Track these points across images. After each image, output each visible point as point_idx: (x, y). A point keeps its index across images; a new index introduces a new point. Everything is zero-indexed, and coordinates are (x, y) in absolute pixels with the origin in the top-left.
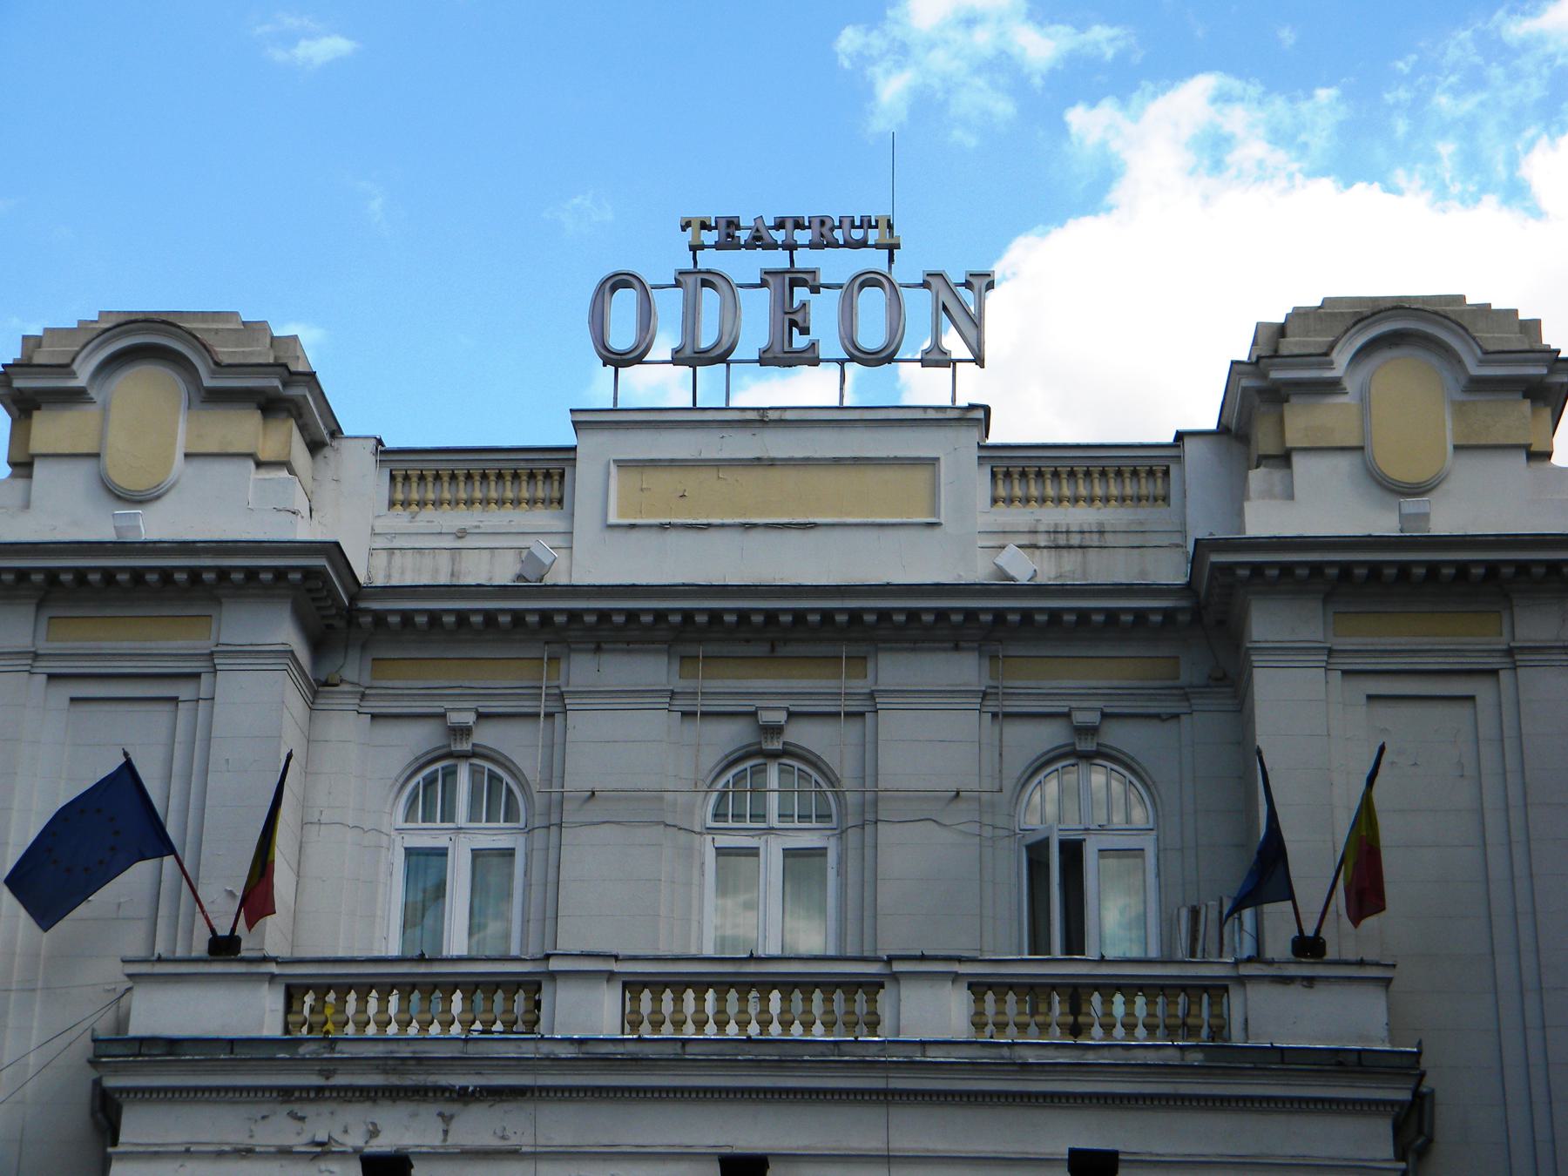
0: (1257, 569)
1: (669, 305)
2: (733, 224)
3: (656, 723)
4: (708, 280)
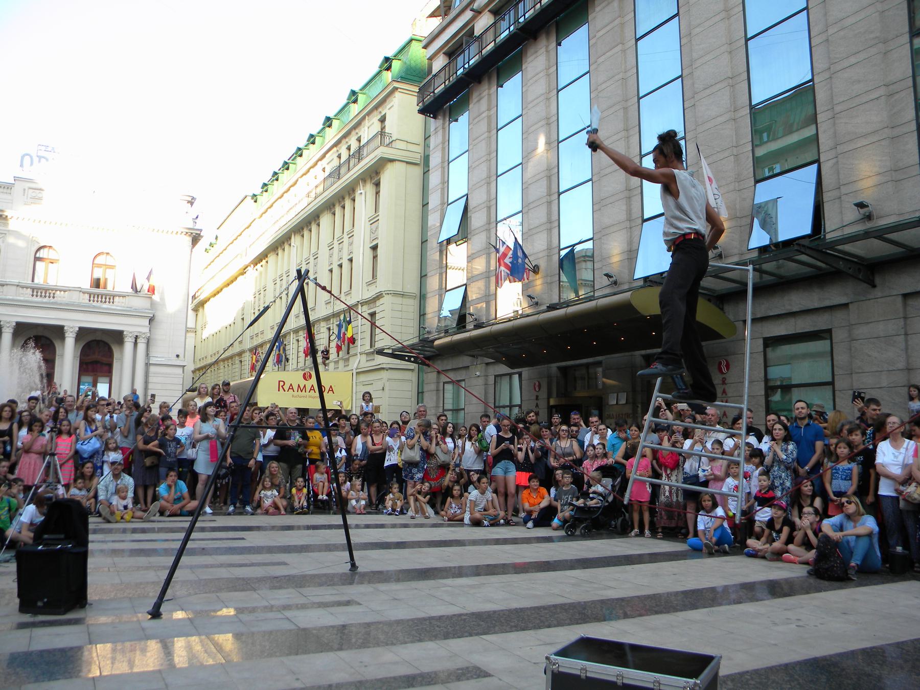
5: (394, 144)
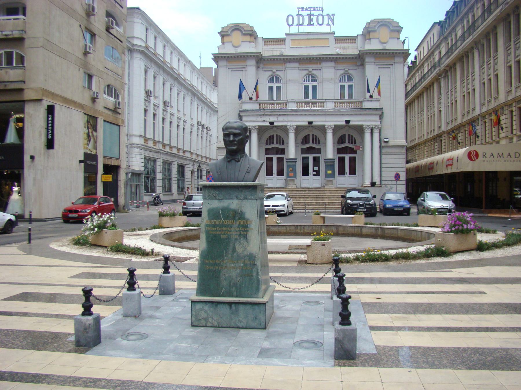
0: (367, 53)
1: (296, 18)
2: (303, 8)
3: (296, 71)
4: (301, 15)
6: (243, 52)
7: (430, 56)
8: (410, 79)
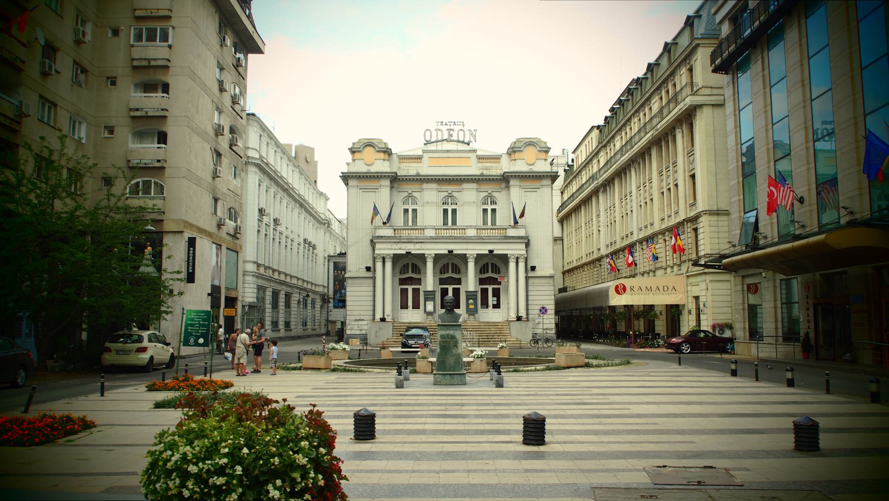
1: (434, 133)
3: (435, 192)
5: (700, 92)
6: (380, 173)
7: (588, 163)
8: (566, 186)
